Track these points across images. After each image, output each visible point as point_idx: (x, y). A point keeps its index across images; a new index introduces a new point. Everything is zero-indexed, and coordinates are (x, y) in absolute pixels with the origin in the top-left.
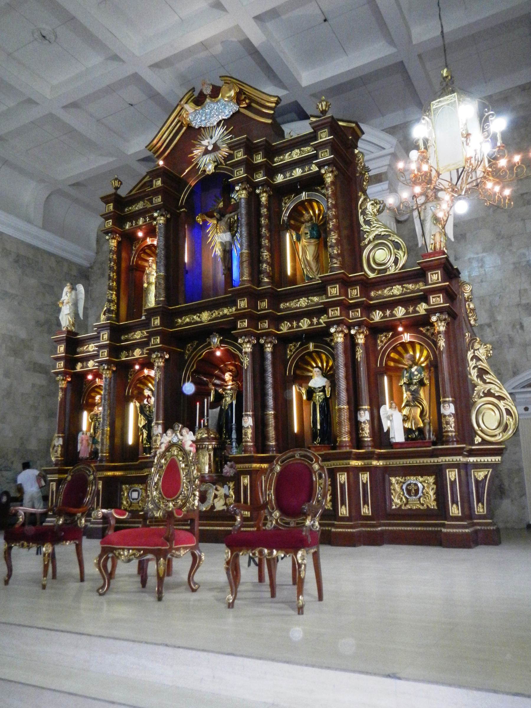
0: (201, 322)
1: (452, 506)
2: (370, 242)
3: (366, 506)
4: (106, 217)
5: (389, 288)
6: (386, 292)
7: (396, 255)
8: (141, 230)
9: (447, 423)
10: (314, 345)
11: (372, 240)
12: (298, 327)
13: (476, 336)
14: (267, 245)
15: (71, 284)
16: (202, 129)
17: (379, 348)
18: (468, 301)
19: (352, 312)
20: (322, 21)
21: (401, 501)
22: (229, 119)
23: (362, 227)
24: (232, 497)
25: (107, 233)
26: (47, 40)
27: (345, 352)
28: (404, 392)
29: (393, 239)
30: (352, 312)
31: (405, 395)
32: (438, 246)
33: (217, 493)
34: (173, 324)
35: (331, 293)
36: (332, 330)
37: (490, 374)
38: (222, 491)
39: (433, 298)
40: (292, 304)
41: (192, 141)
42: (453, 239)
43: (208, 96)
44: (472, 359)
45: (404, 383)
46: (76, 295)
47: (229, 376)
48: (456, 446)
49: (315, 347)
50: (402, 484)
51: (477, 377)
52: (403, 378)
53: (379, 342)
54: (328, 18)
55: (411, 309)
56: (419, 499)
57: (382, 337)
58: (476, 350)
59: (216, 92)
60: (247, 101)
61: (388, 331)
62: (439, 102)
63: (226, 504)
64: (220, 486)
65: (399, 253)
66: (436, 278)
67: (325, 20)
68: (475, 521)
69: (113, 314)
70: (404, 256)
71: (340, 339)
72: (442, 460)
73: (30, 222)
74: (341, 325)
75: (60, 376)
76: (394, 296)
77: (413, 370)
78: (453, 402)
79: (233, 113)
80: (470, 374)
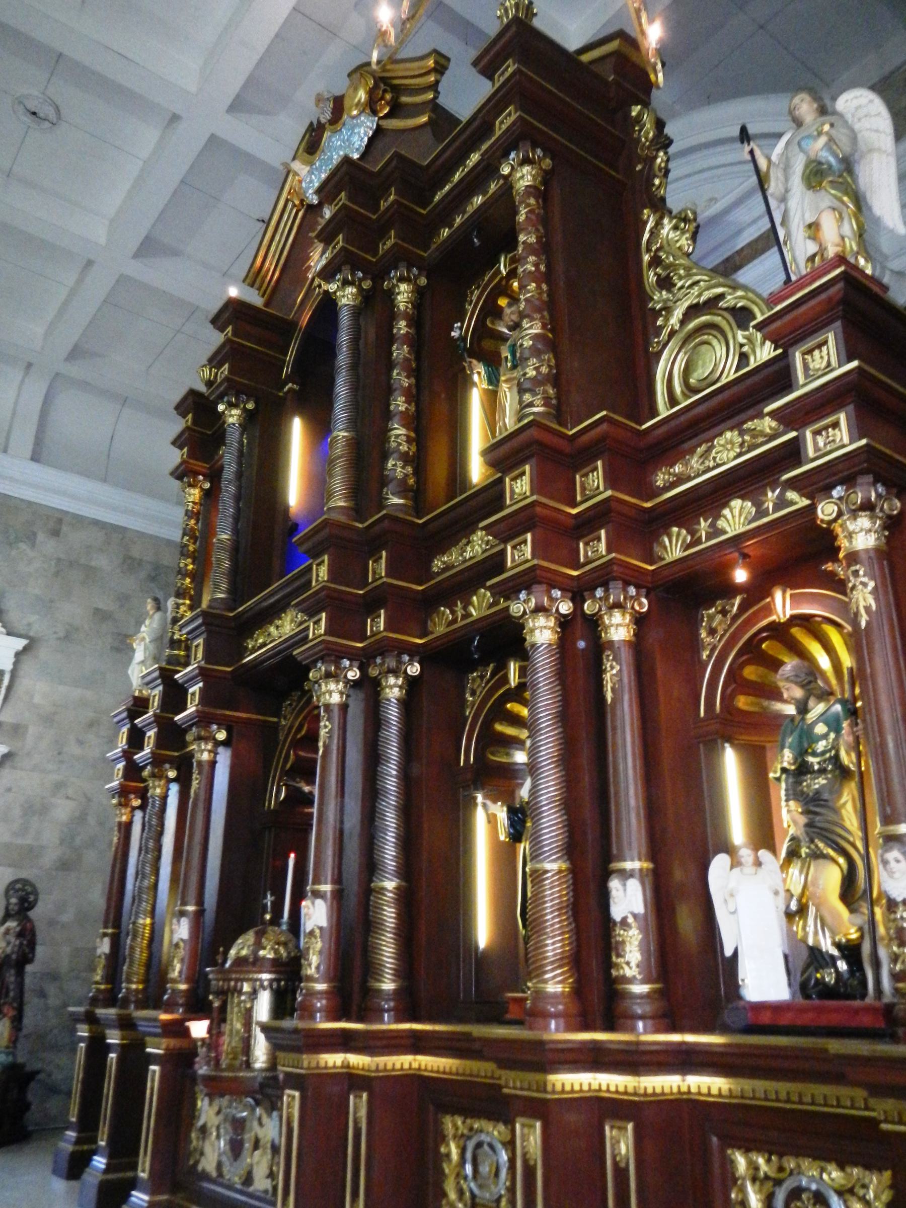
2: (672, 333)
5: (704, 447)
11: (677, 327)
28: (783, 803)
39: (817, 433)
45: (784, 770)
50: (770, 1184)
52: (783, 748)
53: (703, 634)
57: (711, 618)
69: (179, 649)
74: (537, 588)
77: (811, 716)
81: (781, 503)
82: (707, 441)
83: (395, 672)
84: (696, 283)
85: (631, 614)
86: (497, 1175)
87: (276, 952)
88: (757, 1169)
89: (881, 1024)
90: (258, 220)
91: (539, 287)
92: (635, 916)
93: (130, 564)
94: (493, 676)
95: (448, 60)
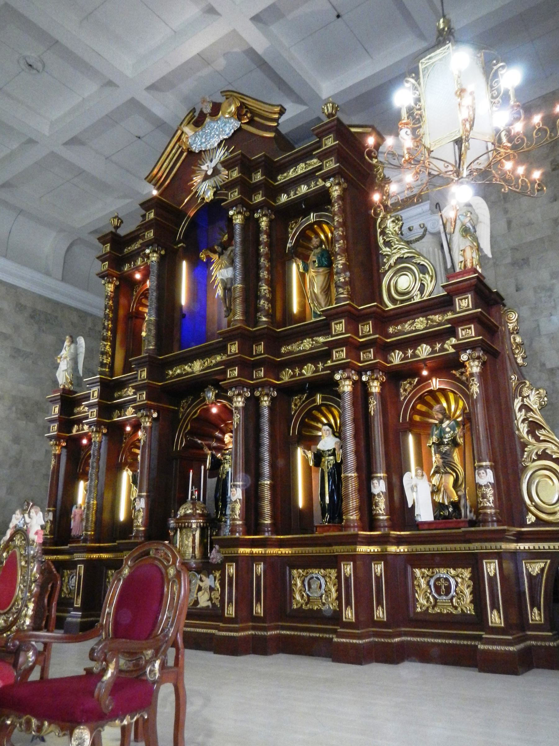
0: (193, 373)
1: (491, 613)
2: (390, 267)
3: (380, 608)
4: (102, 258)
5: (411, 322)
6: (407, 327)
7: (422, 280)
8: (139, 272)
9: (484, 496)
10: (322, 397)
12: (301, 374)
13: (525, 379)
14: (266, 277)
15: (71, 337)
16: (203, 153)
17: (402, 398)
18: (513, 333)
19: (364, 353)
20: (335, 18)
21: (427, 602)
22: (230, 138)
23: (382, 249)
24: (218, 590)
25: (103, 277)
26: (33, 68)
27: (354, 404)
28: (433, 455)
29: (418, 261)
30: (364, 353)
31: (434, 459)
32: (469, 265)
33: (201, 584)
34: (163, 377)
35: (335, 330)
36: (337, 377)
37: (545, 429)
38: (208, 582)
39: (463, 330)
40: (293, 347)
41: (193, 167)
42: (490, 256)
43: (208, 115)
44: (520, 410)
45: (433, 443)
46: (76, 349)
47: (229, 438)
48: (496, 527)
49: (323, 399)
50: (428, 578)
51: (528, 433)
52: (433, 436)
53: (402, 391)
54: (341, 14)
55: (438, 346)
57: (405, 385)
58: (526, 397)
59: (216, 109)
60: (249, 115)
61: (413, 376)
62: (430, 58)
63: (211, 599)
64: (205, 576)
65: (425, 278)
66: (466, 305)
67: (338, 16)
68: (529, 633)
69: (106, 368)
70: (431, 281)
71: (347, 387)
72: (476, 547)
73: (48, 273)
74: (348, 370)
75: (53, 440)
76: (416, 331)
77: (444, 425)
78: (491, 467)
79: (235, 131)
80: (518, 429)
82: (412, 319)
84: (400, 249)
86: (320, 587)
87: (203, 511)
90: (137, 137)
91: (344, 242)
92: (382, 492)
93: (20, 307)
95: (285, 110)
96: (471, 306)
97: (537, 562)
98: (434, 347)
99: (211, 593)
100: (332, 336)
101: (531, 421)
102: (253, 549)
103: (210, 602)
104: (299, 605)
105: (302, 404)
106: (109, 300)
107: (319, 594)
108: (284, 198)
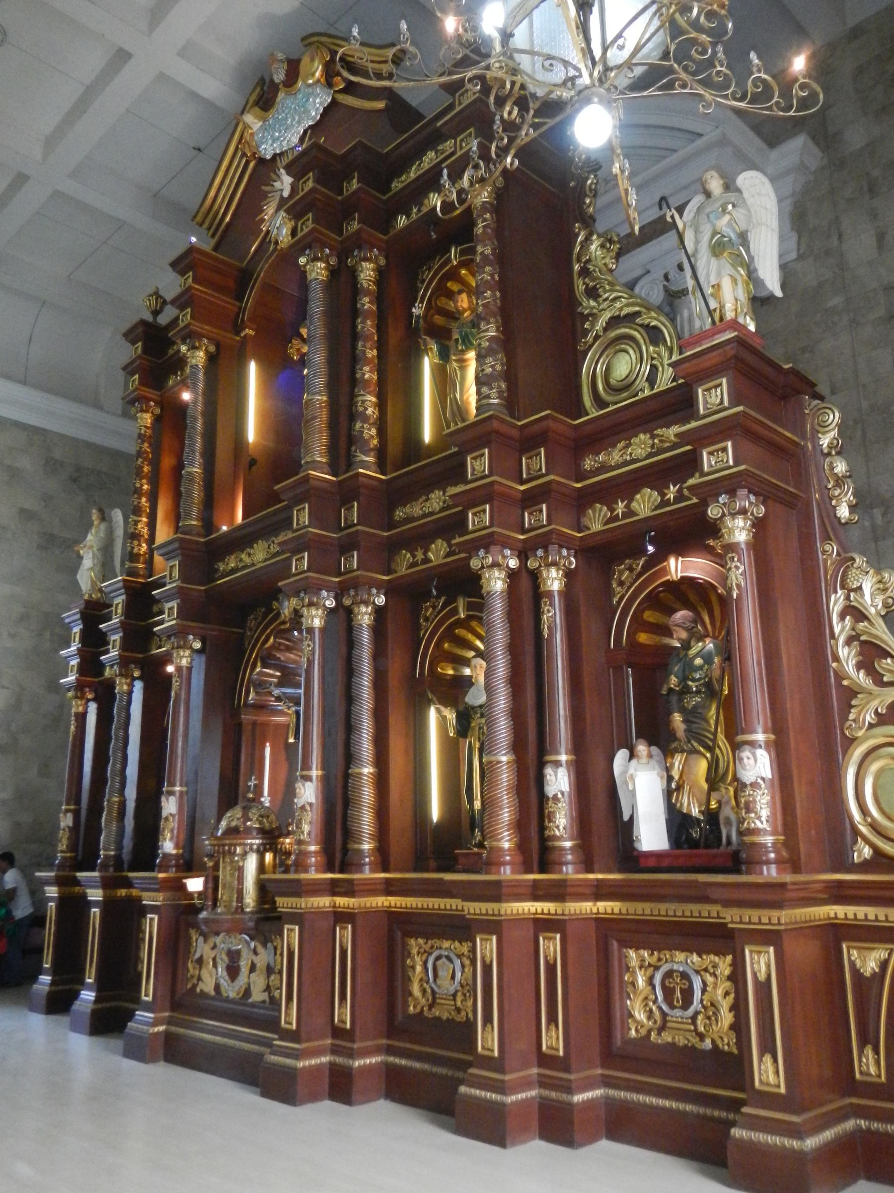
0: (253, 565)
2: (597, 337)
7: (653, 359)
10: (469, 602)
17: (615, 600)
23: (581, 304)
29: (647, 321)
32: (729, 315)
34: (210, 575)
40: (415, 509)
41: (263, 188)
42: (779, 293)
44: (842, 617)
51: (859, 666)
56: (694, 1018)
57: (621, 573)
58: (855, 590)
66: (718, 401)
73: (98, 406)
74: (493, 548)
77: (693, 652)
78: (768, 746)
80: (836, 659)
81: (680, 497)
83: (366, 603)
84: (616, 299)
85: (563, 570)
86: (453, 977)
87: (261, 823)
88: (643, 960)
89: (730, 864)
91: (494, 295)
92: (562, 793)
93: (52, 466)
94: (443, 607)
96: (726, 403)
97: (873, 949)
98: (666, 495)
99: (268, 977)
100: (467, 482)
101: (866, 642)
102: (334, 898)
103: (266, 993)
104: (418, 1009)
105: (436, 617)
106: (143, 442)
107: (452, 990)
108: (402, 221)
